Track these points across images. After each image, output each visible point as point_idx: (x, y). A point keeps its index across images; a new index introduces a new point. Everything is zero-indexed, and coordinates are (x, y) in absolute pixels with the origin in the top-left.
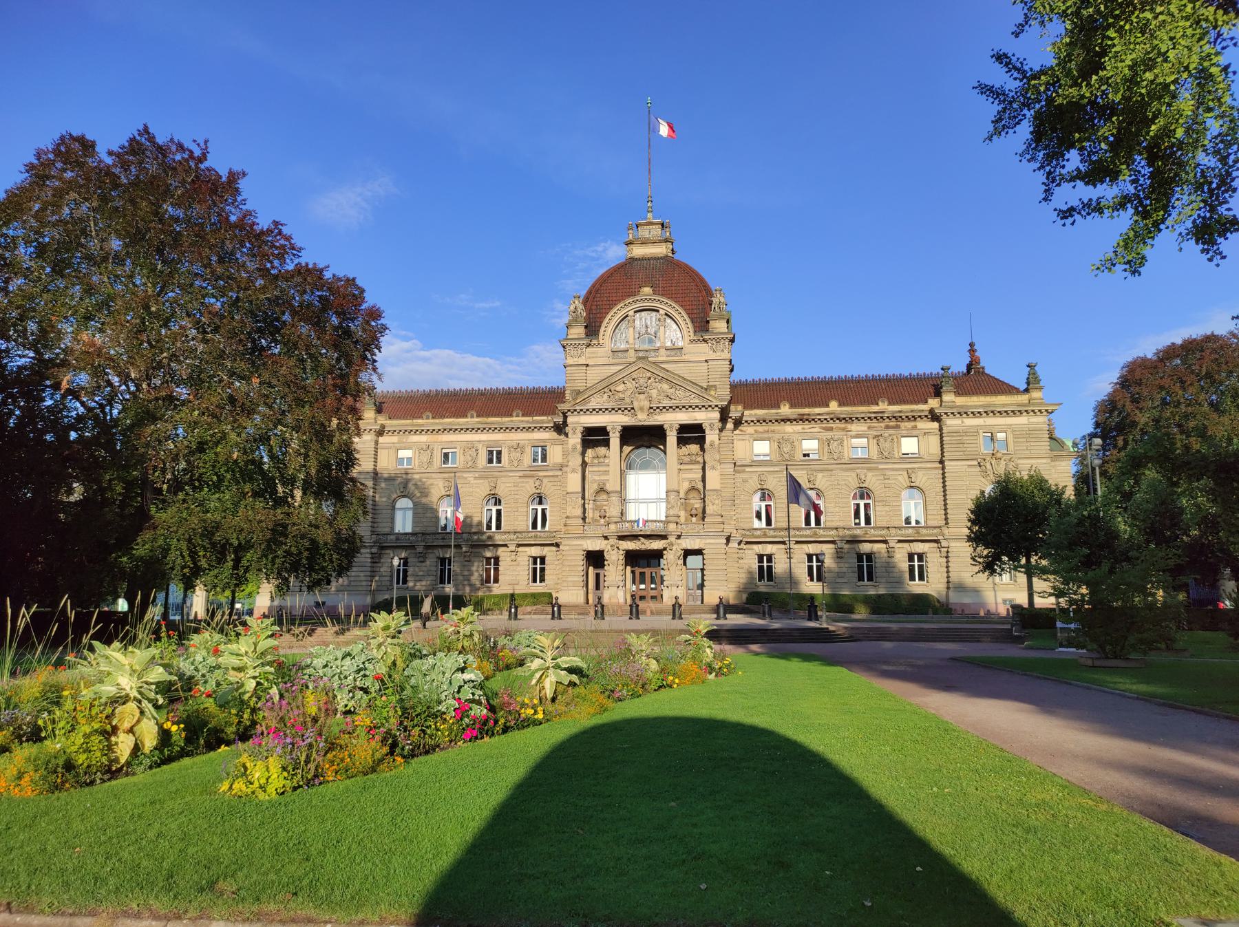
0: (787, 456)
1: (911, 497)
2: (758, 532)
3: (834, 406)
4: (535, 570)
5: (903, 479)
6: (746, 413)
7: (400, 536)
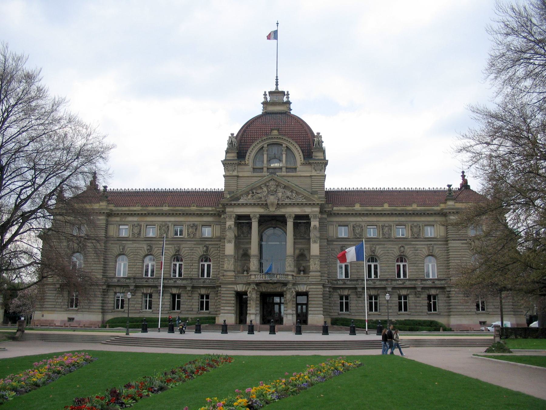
0: (358, 236)
1: (430, 262)
2: (341, 282)
3: (386, 206)
4: (202, 303)
5: (425, 251)
6: (335, 208)
7: (119, 279)
